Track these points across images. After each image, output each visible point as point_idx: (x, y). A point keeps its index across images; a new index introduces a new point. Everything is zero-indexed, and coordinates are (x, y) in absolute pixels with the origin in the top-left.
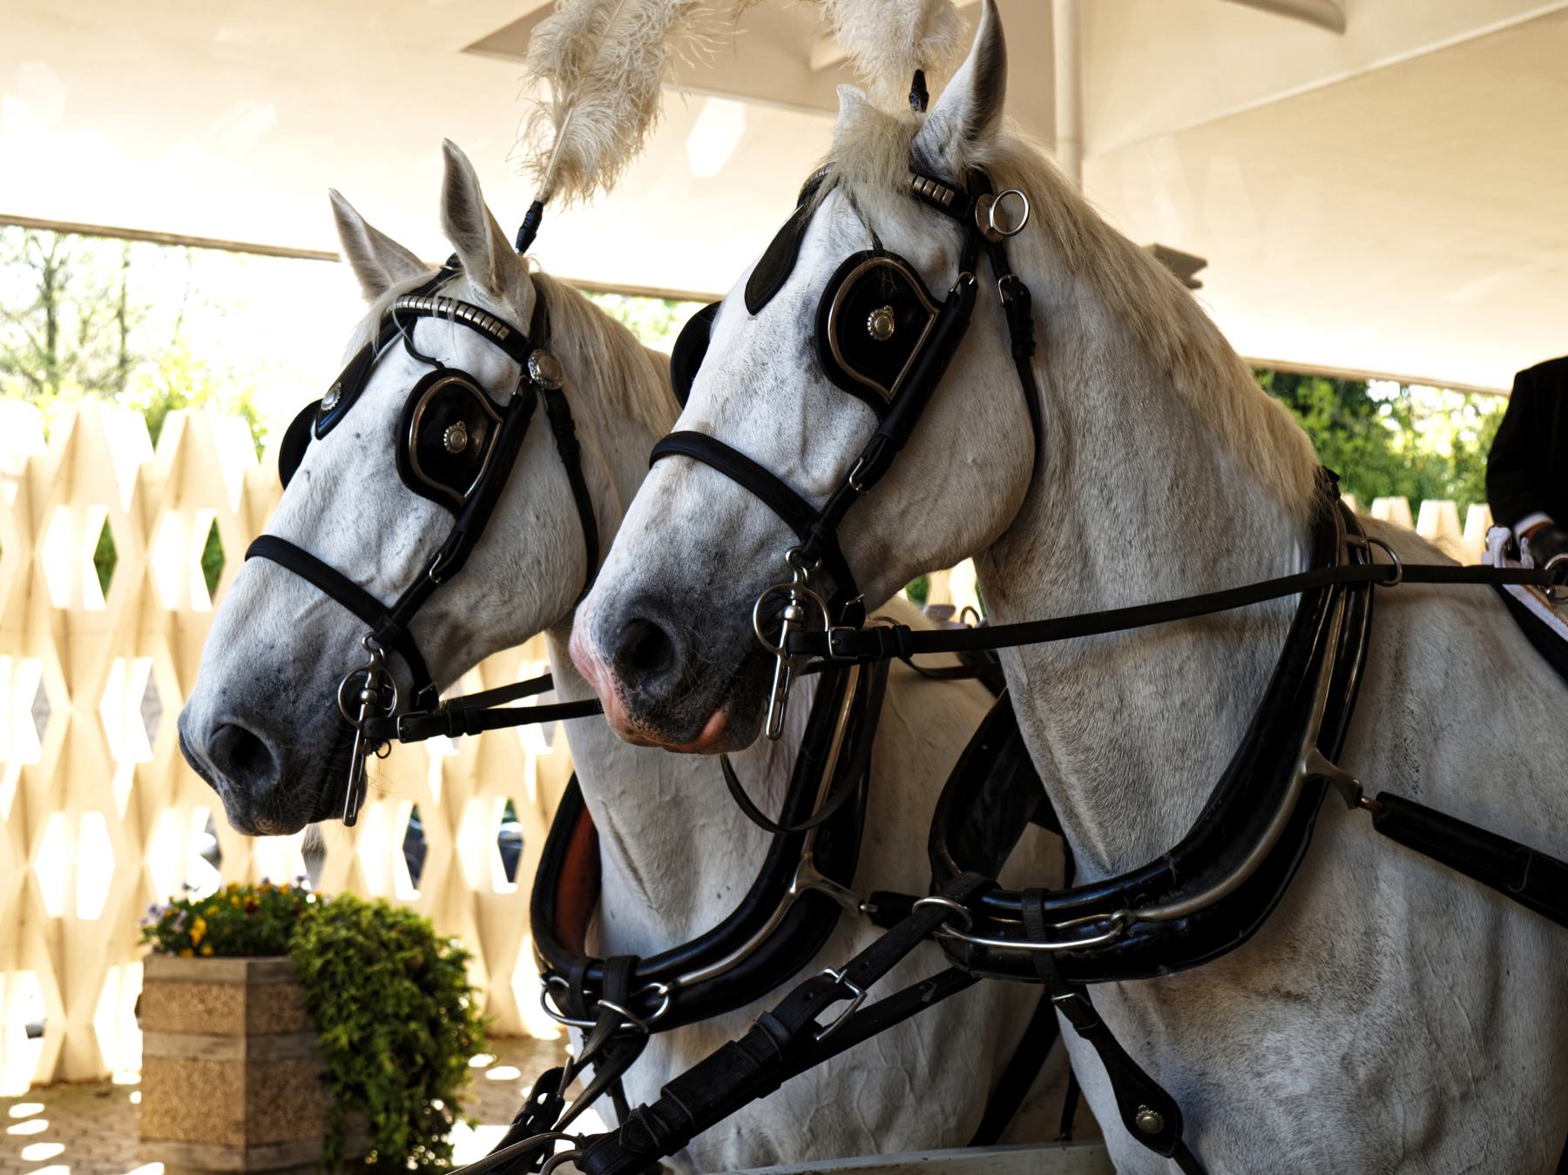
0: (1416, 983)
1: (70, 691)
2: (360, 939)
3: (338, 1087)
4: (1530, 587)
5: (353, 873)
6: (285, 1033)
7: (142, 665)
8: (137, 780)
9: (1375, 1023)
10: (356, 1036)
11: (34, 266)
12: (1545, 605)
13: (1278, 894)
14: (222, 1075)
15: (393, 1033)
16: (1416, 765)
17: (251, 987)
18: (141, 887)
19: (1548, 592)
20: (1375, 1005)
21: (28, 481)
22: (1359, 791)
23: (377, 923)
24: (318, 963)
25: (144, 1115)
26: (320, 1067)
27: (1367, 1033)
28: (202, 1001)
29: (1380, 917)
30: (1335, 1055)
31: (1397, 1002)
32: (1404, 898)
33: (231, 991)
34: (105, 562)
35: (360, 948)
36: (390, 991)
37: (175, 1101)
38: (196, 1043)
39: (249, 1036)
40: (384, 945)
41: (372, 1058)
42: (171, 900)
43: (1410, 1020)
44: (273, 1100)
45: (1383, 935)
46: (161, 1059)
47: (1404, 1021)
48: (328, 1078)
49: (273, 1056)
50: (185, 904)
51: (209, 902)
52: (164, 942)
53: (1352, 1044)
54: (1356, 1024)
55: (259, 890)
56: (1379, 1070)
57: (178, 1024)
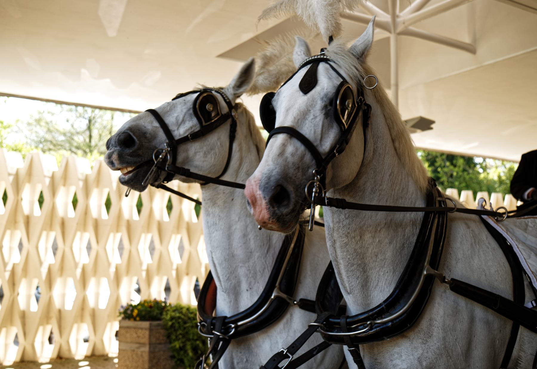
0: (444, 337)
1: (98, 242)
2: (183, 317)
3: (175, 360)
4: (490, 216)
5: (179, 297)
6: (160, 344)
7: (119, 235)
8: (117, 268)
9: (430, 348)
10: (181, 345)
11: (86, 119)
12: (494, 222)
13: (422, 308)
14: (142, 356)
15: (192, 344)
16: (450, 270)
17: (151, 330)
18: (118, 299)
19: (496, 218)
20: (431, 343)
21: (86, 181)
22: (444, 278)
23: (187, 312)
24: (170, 323)
25: (119, 366)
26: (170, 354)
27: (427, 351)
28: (136, 333)
29: (435, 315)
30: (416, 357)
31: (438, 342)
32: (443, 309)
33: (144, 331)
34: (108, 204)
35: (182, 319)
36: (191, 332)
37: (128, 363)
38: (134, 346)
39: (150, 344)
40: (189, 318)
41: (186, 352)
42: (128, 304)
43: (442, 348)
44: (157, 363)
45: (435, 321)
46: (124, 350)
47: (440, 349)
48: (173, 357)
49: (157, 350)
50: (131, 305)
51: (138, 305)
52: (125, 316)
53: (422, 354)
54: (424, 348)
55: (154, 301)
56: (430, 363)
57: (129, 340)
